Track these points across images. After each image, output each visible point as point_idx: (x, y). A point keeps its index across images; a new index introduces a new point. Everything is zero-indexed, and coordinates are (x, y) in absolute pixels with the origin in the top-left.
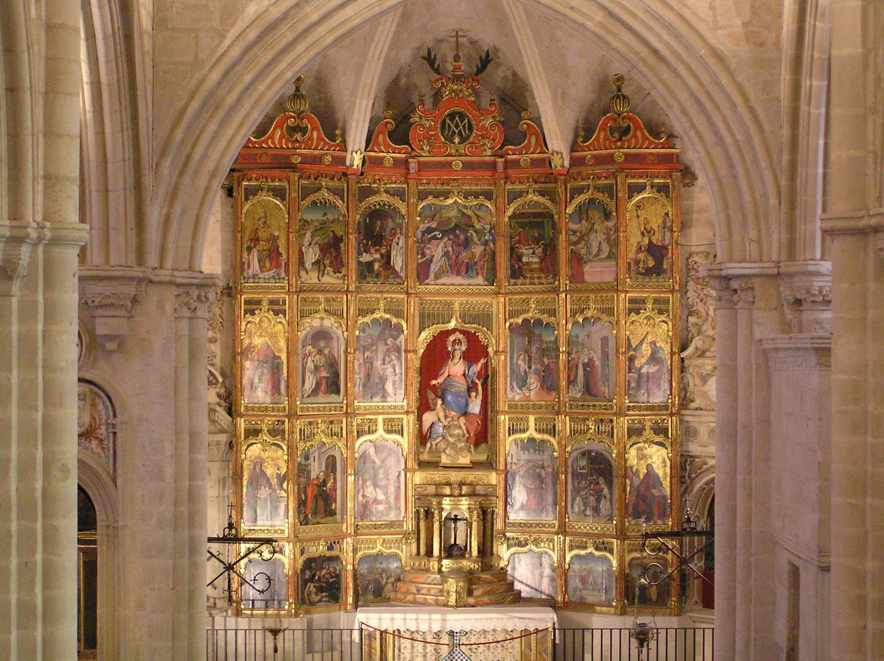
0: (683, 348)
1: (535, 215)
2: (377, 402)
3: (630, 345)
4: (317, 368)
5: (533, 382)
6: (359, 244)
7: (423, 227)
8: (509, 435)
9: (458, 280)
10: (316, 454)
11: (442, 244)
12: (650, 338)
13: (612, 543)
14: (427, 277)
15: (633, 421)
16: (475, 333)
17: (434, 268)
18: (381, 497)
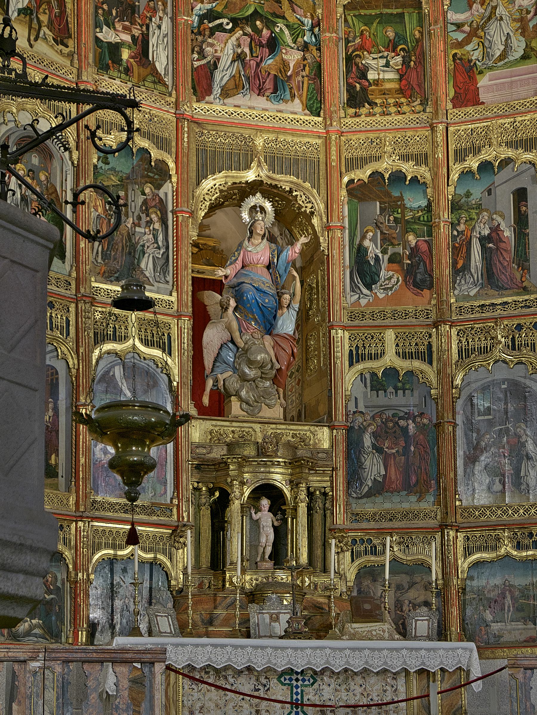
8: (351, 364)
9: (261, 102)
14: (209, 91)
16: (291, 191)
17: (222, 77)
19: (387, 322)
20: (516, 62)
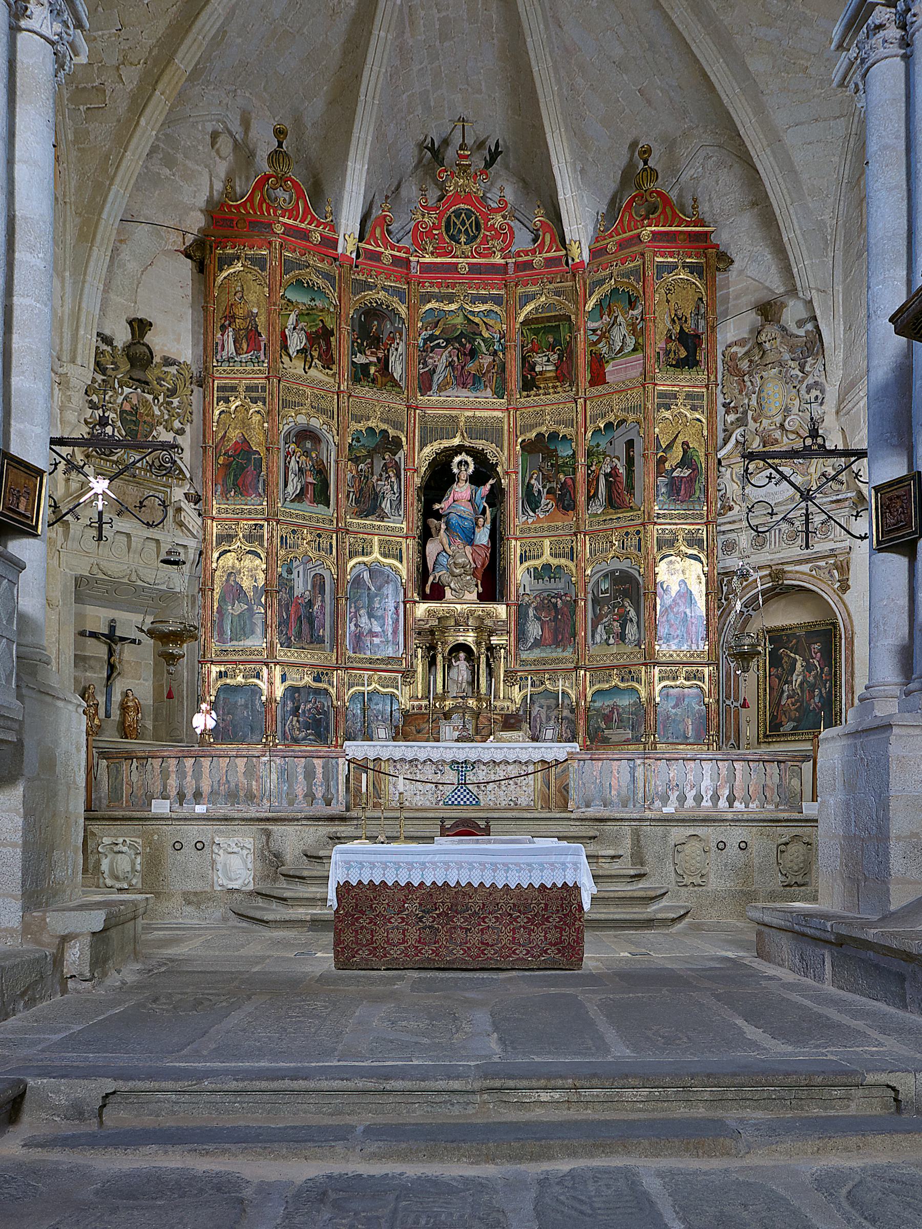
1: (549, 319)
3: (659, 446)
6: (353, 342)
8: (521, 563)
9: (465, 392)
10: (301, 569)
13: (640, 671)
15: (663, 530)
17: (437, 378)
19: (544, 534)
20: (629, 353)
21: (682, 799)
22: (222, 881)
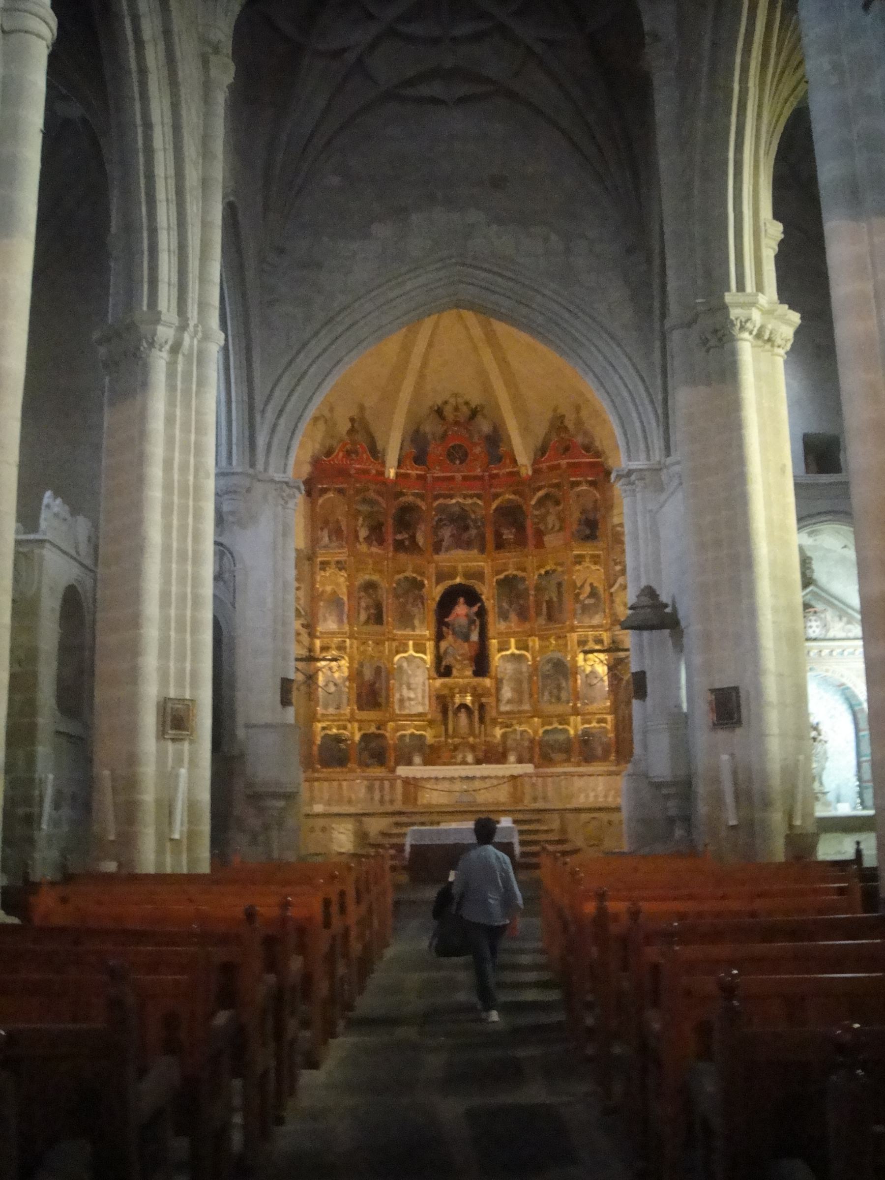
0: (611, 586)
2: (408, 632)
4: (367, 608)
5: (513, 616)
7: (436, 518)
11: (450, 529)
12: (589, 581)
17: (445, 544)
18: (412, 695)
21: (587, 796)
22: (336, 848)
